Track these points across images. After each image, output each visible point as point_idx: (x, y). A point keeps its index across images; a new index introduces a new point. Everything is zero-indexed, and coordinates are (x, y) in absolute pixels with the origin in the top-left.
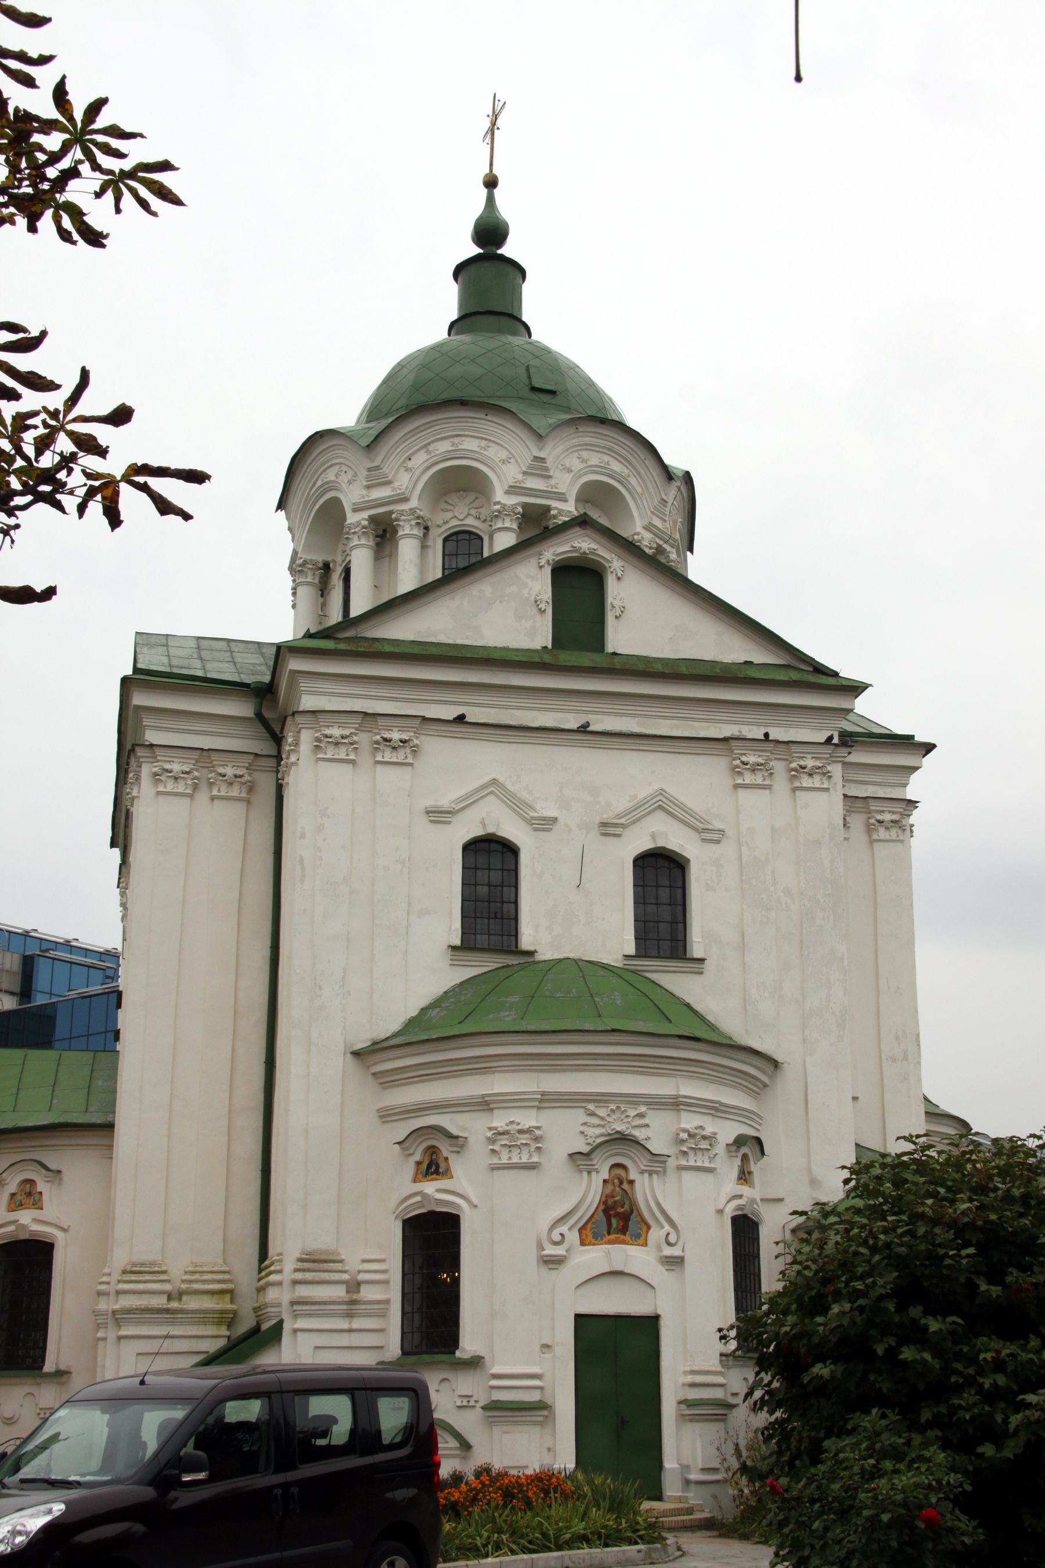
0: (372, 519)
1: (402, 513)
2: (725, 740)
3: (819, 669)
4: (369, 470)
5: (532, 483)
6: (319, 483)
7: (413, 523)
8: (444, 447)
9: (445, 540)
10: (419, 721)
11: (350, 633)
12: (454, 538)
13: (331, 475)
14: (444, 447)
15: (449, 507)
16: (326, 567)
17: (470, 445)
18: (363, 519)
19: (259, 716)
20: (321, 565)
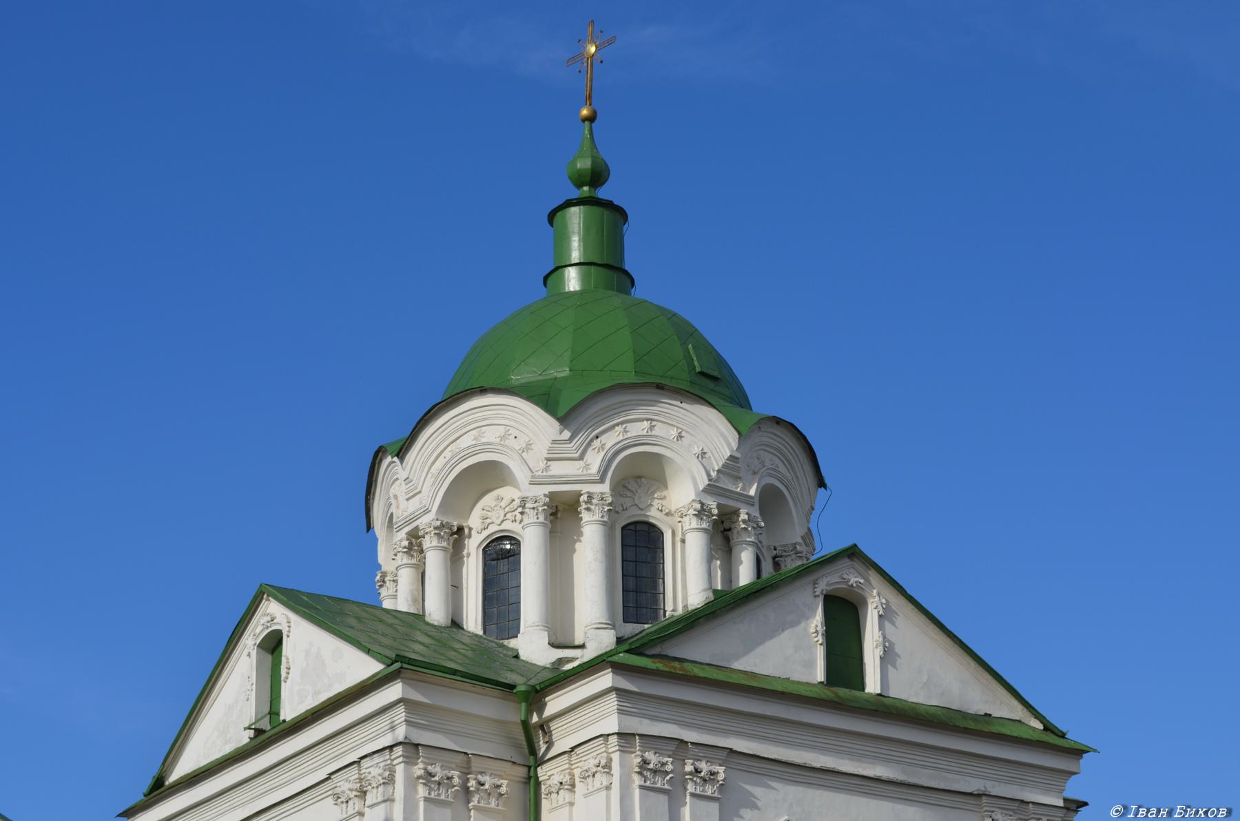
0: (552, 495)
1: (590, 496)
2: (979, 796)
3: (1048, 728)
4: (554, 442)
5: (727, 484)
6: (466, 441)
7: (607, 508)
8: (638, 429)
9: (623, 528)
10: (726, 753)
11: (656, 651)
12: (632, 527)
13: (491, 435)
14: (638, 429)
15: (629, 494)
16: (460, 530)
17: (659, 430)
18: (545, 495)
19: (525, 724)
20: (455, 529)
